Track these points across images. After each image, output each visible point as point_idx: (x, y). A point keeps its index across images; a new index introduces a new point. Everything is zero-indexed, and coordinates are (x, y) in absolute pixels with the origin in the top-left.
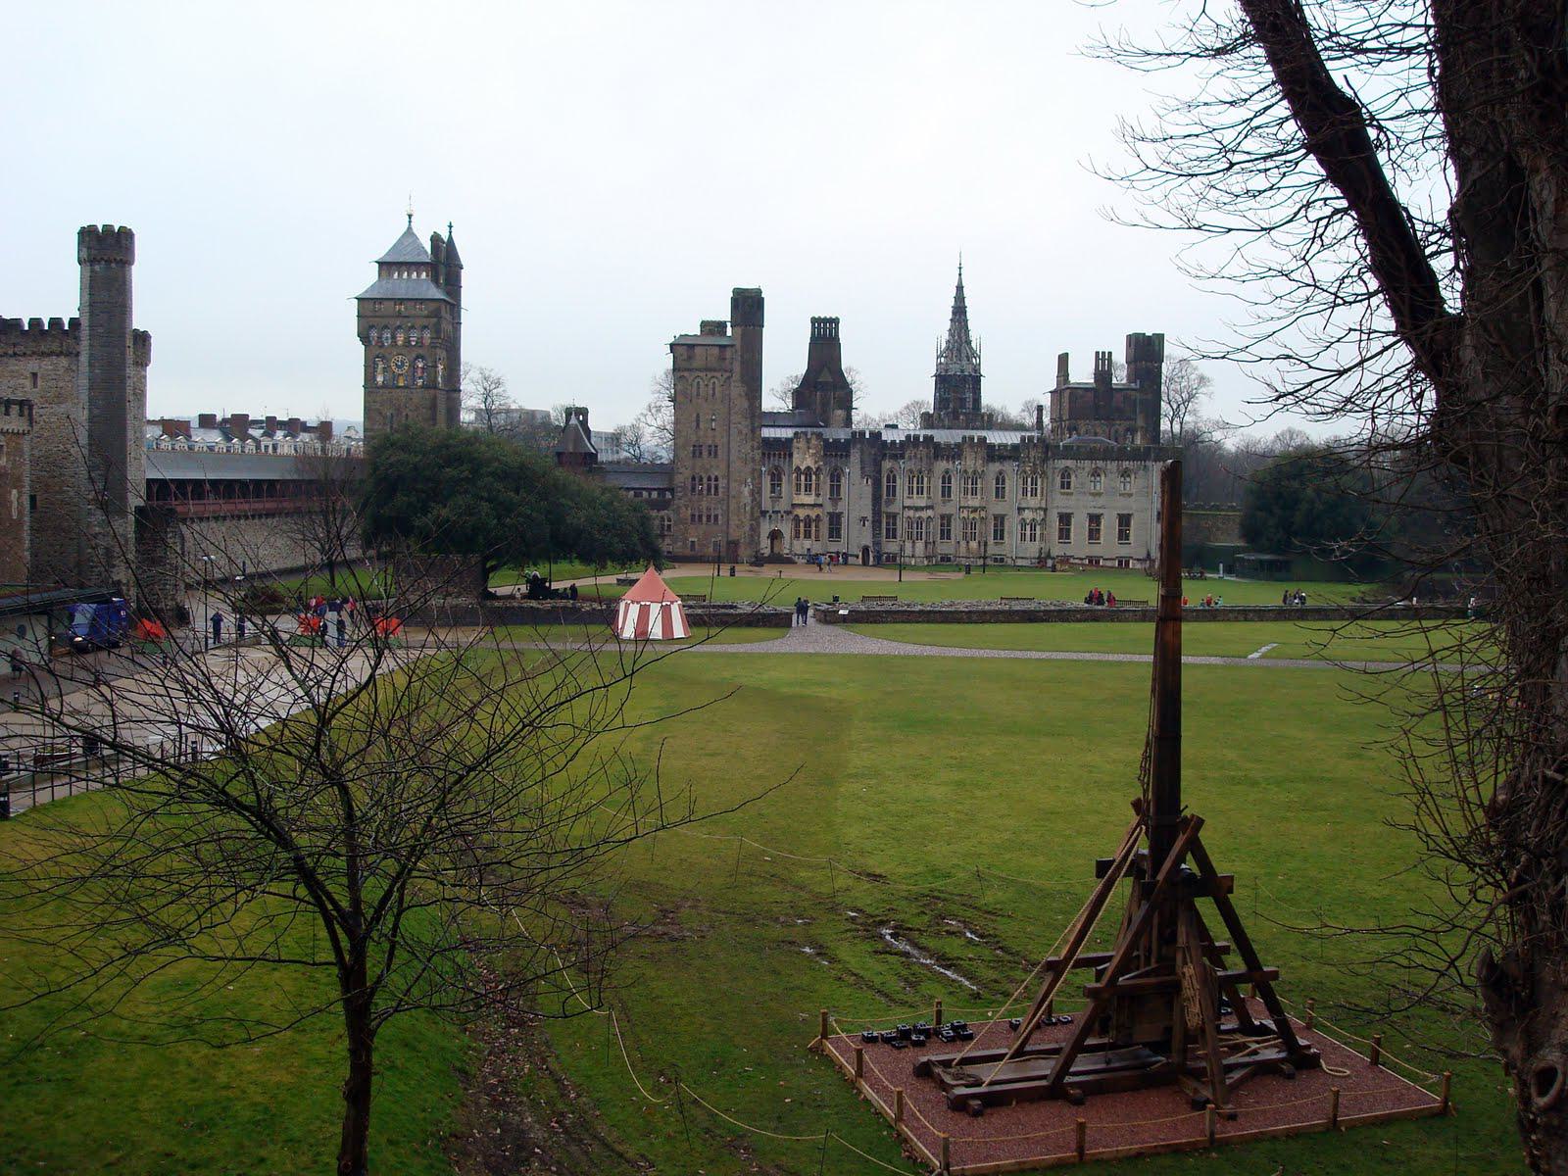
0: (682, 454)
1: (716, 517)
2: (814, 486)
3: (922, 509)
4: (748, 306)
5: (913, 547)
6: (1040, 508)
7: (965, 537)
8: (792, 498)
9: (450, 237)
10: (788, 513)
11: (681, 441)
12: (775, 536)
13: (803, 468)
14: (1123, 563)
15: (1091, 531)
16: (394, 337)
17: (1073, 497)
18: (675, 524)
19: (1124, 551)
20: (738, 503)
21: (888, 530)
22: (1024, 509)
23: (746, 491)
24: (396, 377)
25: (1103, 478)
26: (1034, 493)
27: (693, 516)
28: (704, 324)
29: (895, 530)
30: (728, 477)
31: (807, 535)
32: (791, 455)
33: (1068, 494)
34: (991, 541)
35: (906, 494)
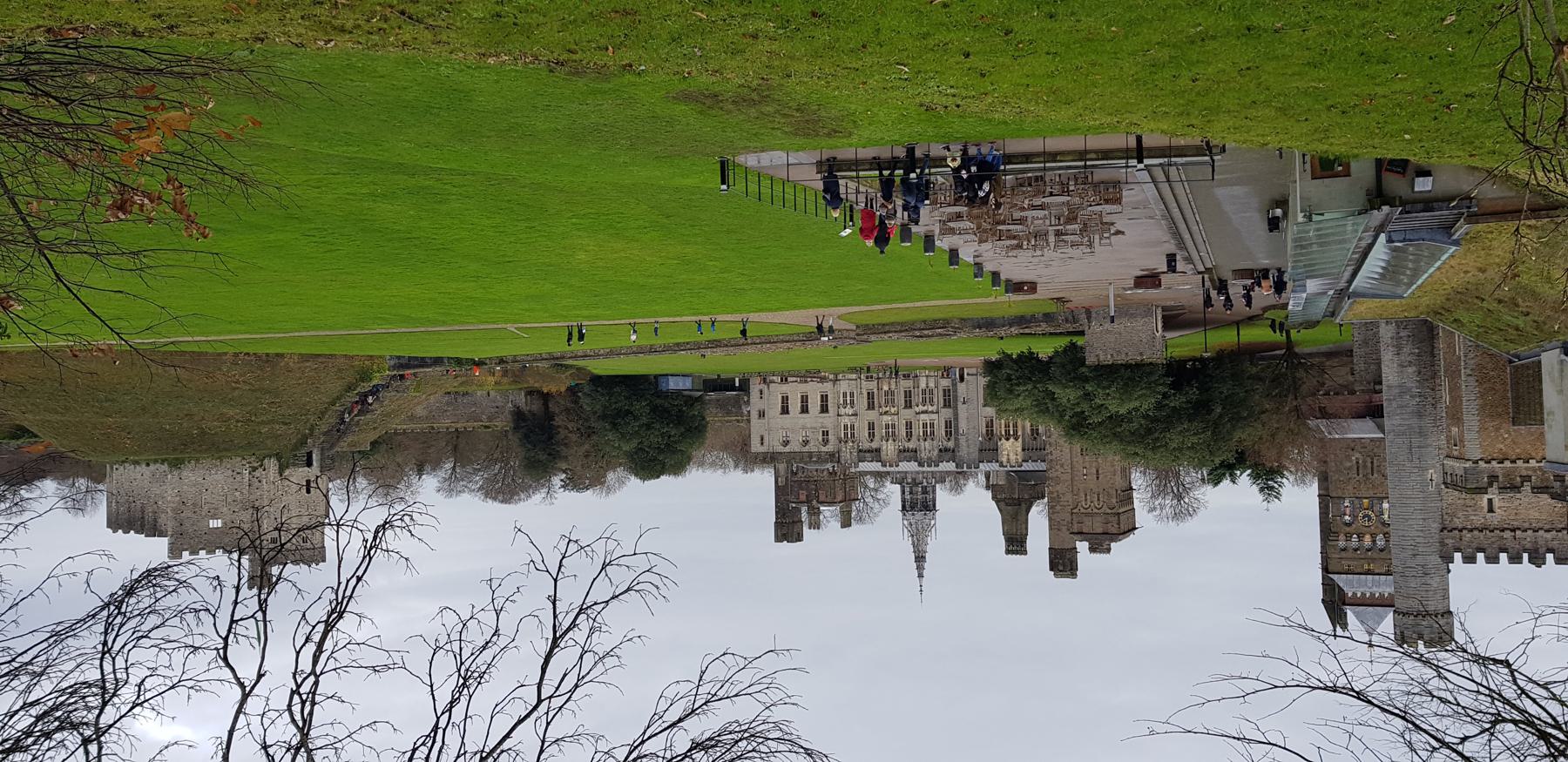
2: (1003, 426)
3: (923, 412)
4: (1062, 563)
6: (841, 416)
7: (893, 393)
13: (1012, 440)
14: (784, 380)
15: (807, 402)
16: (1374, 541)
19: (785, 388)
22: (852, 415)
24: (1371, 507)
25: (801, 440)
28: (1108, 550)
29: (945, 396)
32: (1023, 450)
34: (875, 391)
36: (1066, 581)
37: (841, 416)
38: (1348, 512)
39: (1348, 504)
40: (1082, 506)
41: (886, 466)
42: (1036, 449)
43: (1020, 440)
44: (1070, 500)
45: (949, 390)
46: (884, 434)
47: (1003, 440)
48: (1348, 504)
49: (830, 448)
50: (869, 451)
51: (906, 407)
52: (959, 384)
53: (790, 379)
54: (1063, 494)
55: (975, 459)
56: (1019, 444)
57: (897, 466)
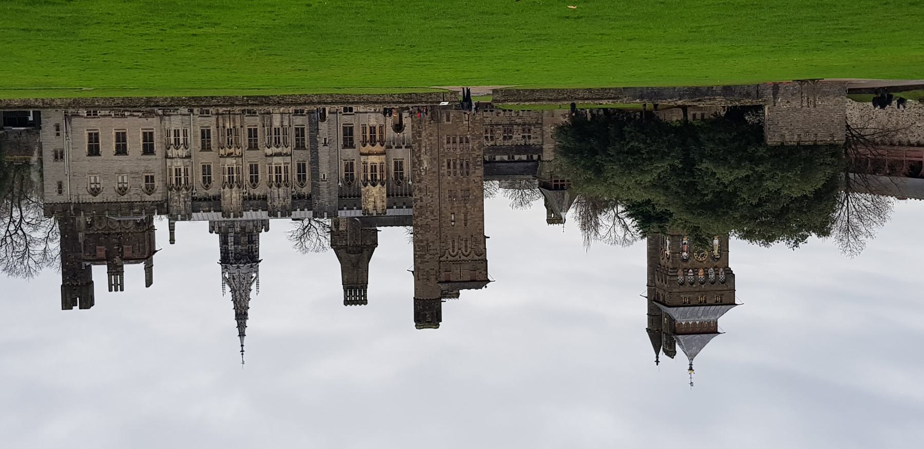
0: (477, 192)
1: (448, 142)
2: (369, 170)
3: (277, 155)
5: (282, 122)
6: (170, 158)
9: (657, 352)
10: (390, 147)
11: (478, 204)
12: (399, 127)
13: (379, 186)
14: (92, 114)
15: (124, 140)
17: (143, 170)
19: (93, 124)
21: (303, 135)
22: (186, 157)
23: (425, 165)
26: (178, 171)
27: (467, 142)
31: (373, 129)
32: (388, 196)
34: (213, 129)
35: (289, 166)
36: (428, 332)
37: (172, 158)
38: (686, 250)
39: (687, 242)
40: (449, 253)
41: (229, 216)
42: (402, 195)
43: (385, 185)
44: (439, 248)
45: (303, 130)
46: (227, 180)
47: (369, 186)
48: (687, 242)
49: (157, 196)
51: (250, 148)
54: (433, 242)
56: (384, 190)
57: (242, 216)
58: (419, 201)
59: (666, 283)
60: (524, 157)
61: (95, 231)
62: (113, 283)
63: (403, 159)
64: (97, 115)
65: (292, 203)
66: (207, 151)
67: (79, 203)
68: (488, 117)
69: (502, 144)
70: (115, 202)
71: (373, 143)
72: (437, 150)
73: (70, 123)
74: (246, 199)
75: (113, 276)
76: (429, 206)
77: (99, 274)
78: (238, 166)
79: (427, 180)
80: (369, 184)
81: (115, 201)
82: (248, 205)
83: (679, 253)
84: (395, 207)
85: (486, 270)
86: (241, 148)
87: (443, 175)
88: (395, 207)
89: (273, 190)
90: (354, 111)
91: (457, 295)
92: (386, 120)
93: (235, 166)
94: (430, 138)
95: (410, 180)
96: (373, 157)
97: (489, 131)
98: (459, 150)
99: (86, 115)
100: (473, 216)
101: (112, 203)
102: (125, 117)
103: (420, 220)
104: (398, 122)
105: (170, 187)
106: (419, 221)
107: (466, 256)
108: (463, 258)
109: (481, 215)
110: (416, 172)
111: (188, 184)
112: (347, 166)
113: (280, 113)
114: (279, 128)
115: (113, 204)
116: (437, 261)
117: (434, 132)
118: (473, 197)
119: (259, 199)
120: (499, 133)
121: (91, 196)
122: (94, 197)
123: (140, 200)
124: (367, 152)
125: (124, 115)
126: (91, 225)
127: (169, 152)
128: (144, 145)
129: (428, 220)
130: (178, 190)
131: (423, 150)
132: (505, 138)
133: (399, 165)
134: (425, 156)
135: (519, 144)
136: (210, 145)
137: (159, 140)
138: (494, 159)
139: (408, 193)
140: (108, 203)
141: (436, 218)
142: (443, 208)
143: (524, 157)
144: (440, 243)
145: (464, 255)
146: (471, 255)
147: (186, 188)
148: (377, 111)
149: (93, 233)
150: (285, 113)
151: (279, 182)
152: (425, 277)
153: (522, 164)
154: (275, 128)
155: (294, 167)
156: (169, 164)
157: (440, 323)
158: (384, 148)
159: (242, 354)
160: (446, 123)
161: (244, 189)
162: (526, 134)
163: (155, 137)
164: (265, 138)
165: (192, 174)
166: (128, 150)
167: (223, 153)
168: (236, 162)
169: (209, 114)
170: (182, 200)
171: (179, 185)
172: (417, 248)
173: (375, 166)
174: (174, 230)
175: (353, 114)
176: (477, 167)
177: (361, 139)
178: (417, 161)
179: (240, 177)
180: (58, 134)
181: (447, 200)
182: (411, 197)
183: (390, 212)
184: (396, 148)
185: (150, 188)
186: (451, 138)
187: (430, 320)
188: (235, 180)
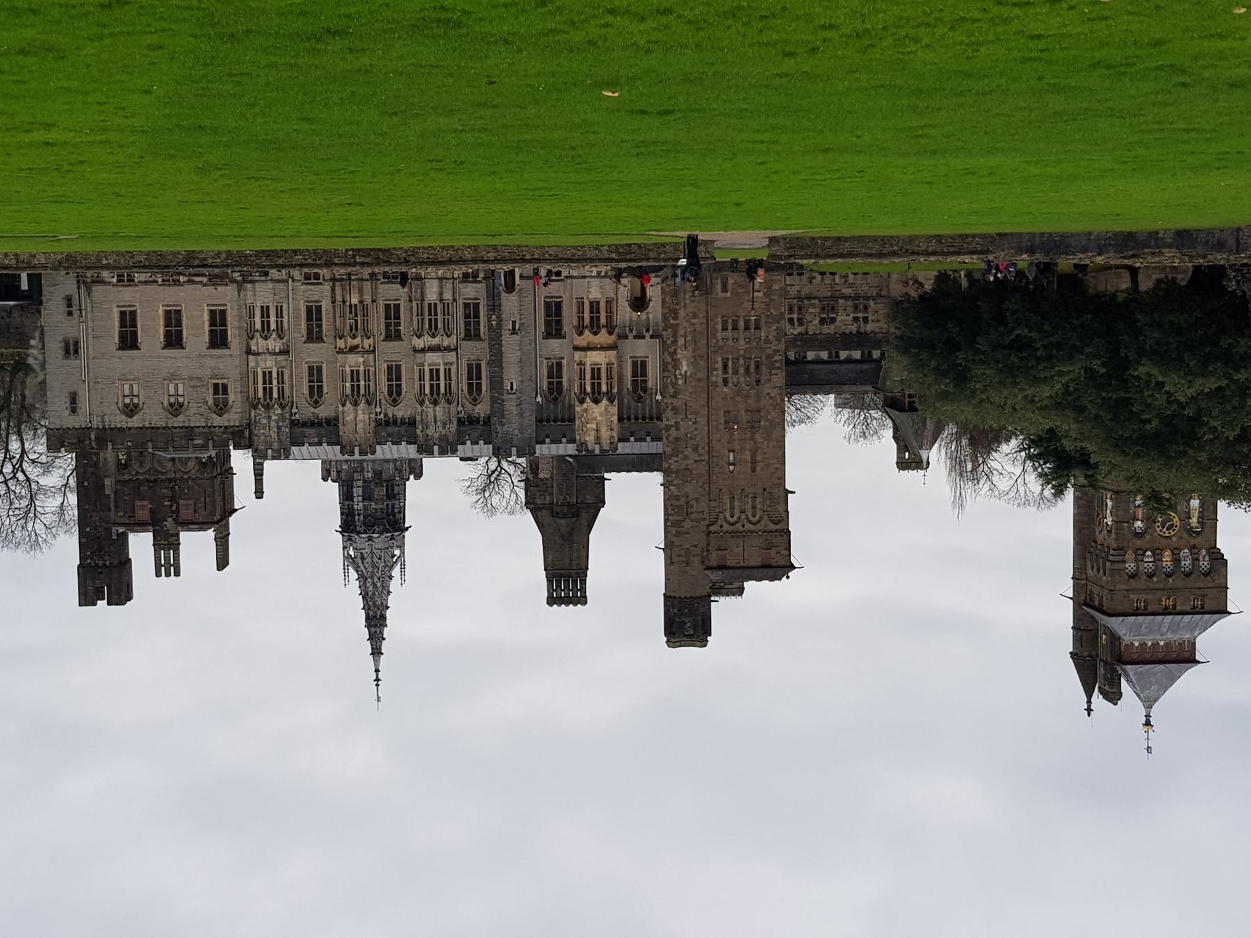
0: (773, 415)
1: (725, 329)
2: (588, 376)
3: (432, 349)
5: (441, 294)
6: (258, 354)
7: (365, 309)
8: (619, 358)
10: (623, 337)
11: (775, 434)
12: (639, 303)
13: (605, 402)
14: (126, 280)
15: (179, 324)
17: (209, 372)
18: (782, 314)
19: (128, 295)
20: (694, 350)
21: (477, 316)
23: (684, 367)
25: (166, 403)
27: (758, 328)
30: (709, 386)
31: (595, 306)
32: (620, 419)
33: (216, 376)
34: (326, 305)
35: (454, 368)
36: (689, 653)
37: (258, 354)
40: (725, 518)
41: (352, 453)
42: (644, 419)
43: (616, 401)
45: (477, 306)
46: (348, 391)
47: (588, 403)
49: (232, 418)
50: (312, 424)
51: (388, 337)
52: (504, 295)
53: (138, 277)
55: (530, 438)
56: (614, 410)
57: (373, 452)
58: (673, 429)
59: (1105, 574)
60: (857, 355)
61: (133, 476)
62: (163, 563)
63: (648, 357)
64: (133, 281)
65: (457, 430)
66: (315, 342)
67: (104, 428)
68: (793, 285)
69: (817, 332)
70: (164, 428)
71: (595, 329)
72: (705, 342)
73: (89, 295)
74: (381, 424)
75: (162, 552)
76: (691, 438)
77: (141, 546)
78: (367, 368)
79: (688, 394)
80: (588, 400)
81: (164, 425)
82: (384, 434)
83: (1129, 522)
84: (632, 439)
85: (789, 548)
86: (372, 339)
87: (715, 385)
88: (632, 439)
89: (425, 409)
90: (563, 274)
91: (740, 591)
92: (617, 289)
93: (362, 368)
94: (693, 321)
95: (659, 394)
96: (594, 353)
97: (796, 309)
98: (742, 342)
99: (115, 280)
100: (767, 456)
101: (158, 428)
102: (179, 285)
103: (675, 461)
104: (638, 294)
105: (255, 403)
106: (673, 463)
107: (755, 524)
108: (748, 526)
109: (781, 453)
110: (669, 380)
111: (283, 398)
112: (550, 368)
113: (439, 279)
114: (435, 304)
115: (160, 431)
116: (703, 532)
117: (699, 310)
118: (768, 423)
119: (403, 423)
120: (813, 313)
121: (123, 417)
122: (129, 420)
123: (204, 425)
124: (586, 344)
125: (179, 281)
126: (126, 466)
127: (253, 342)
128: (211, 332)
129: (689, 462)
130: (268, 407)
131: (681, 342)
132: (823, 321)
133: (640, 368)
134: (685, 352)
135: (847, 332)
136: (321, 331)
137: (236, 323)
138: (805, 357)
139: (655, 416)
140: (153, 428)
141: (702, 458)
142: (714, 442)
143: (857, 355)
144: (710, 500)
145: (750, 522)
146: (763, 523)
147: (281, 403)
148: (603, 274)
149: (130, 480)
150: (446, 279)
151: (435, 396)
152: (683, 559)
153: (852, 366)
154: (430, 304)
155: (461, 368)
156: (252, 364)
157: (709, 638)
158: (613, 337)
159: (377, 685)
160: (721, 295)
161: (378, 406)
162: (860, 315)
163: (229, 318)
164: (412, 320)
165: (292, 380)
166: (185, 340)
167: (342, 346)
168: (364, 362)
169: (319, 279)
170: (273, 424)
171: (268, 400)
172: (670, 509)
173: (599, 369)
174: (262, 475)
175: (562, 280)
176: (773, 372)
177: (575, 322)
178: (670, 360)
179: (371, 386)
180: (70, 314)
181: (721, 427)
182: (659, 423)
183: (623, 448)
184: (635, 337)
185: (221, 405)
186: (730, 321)
187: (692, 633)
188: (362, 391)
